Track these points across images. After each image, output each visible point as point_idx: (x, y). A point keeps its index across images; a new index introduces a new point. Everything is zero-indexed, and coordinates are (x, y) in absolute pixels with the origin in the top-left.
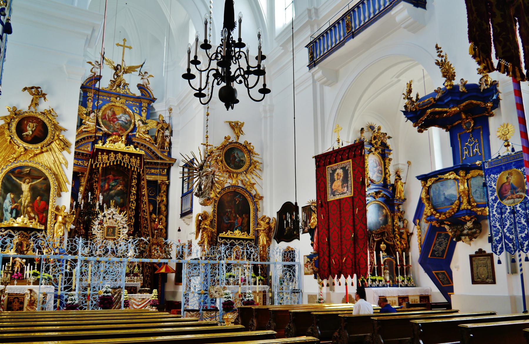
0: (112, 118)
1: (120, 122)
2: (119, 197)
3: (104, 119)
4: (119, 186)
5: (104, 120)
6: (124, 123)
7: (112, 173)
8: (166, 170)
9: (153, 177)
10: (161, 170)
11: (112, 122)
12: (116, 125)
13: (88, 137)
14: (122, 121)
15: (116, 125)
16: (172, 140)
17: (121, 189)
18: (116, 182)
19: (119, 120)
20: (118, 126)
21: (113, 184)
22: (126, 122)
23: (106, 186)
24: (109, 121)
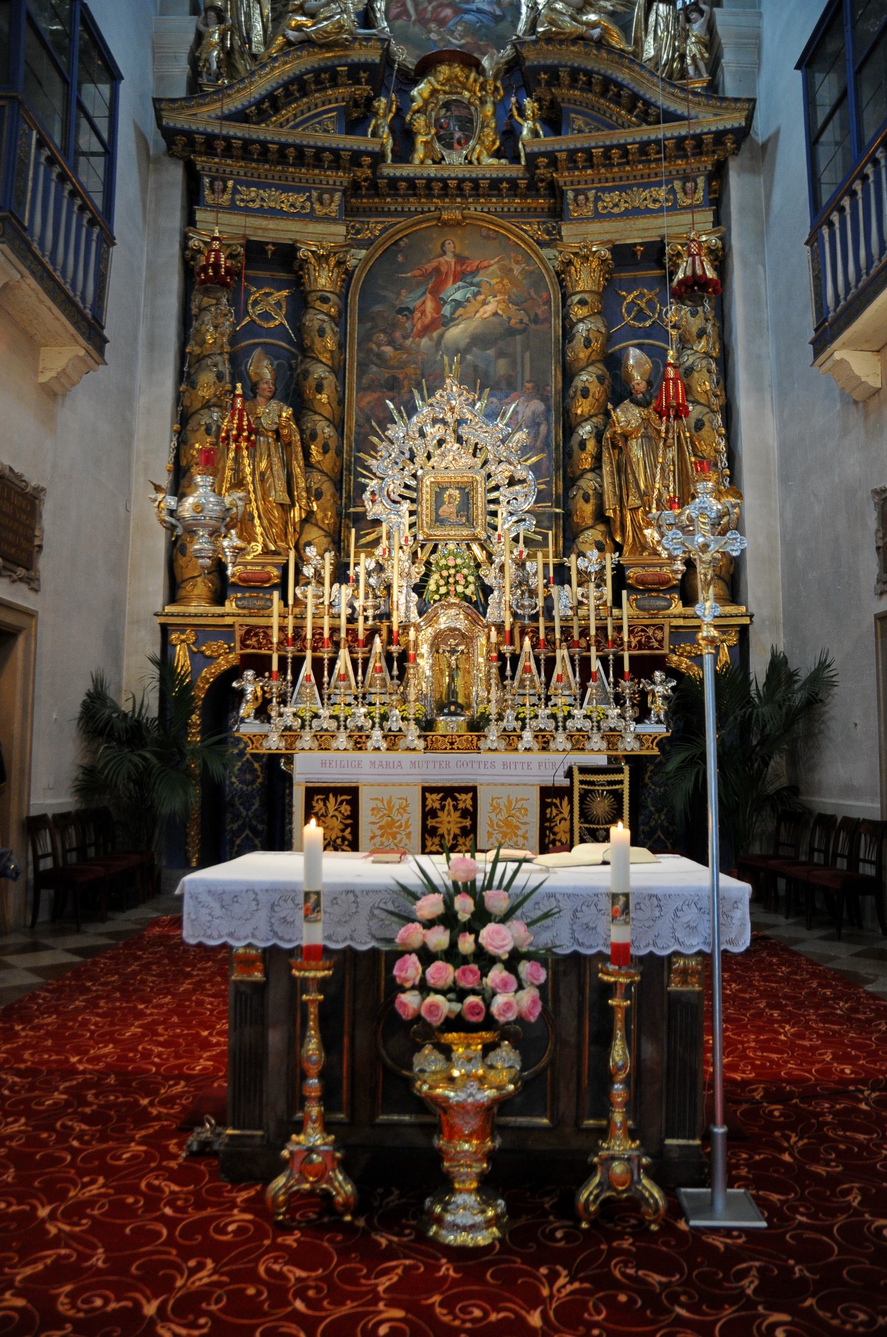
0: (434, 9)
1: (467, 17)
2: (491, 352)
3: (398, 17)
4: (484, 303)
5: (399, 22)
6: (485, 19)
7: (449, 247)
8: (701, 181)
9: (641, 223)
10: (677, 185)
11: (433, 26)
12: (452, 33)
13: (317, 72)
14: (479, 11)
15: (452, 33)
16: (720, 29)
17: (495, 314)
18: (472, 284)
19: (467, 11)
20: (462, 37)
21: (458, 296)
22: (498, 12)
23: (429, 305)
24: (422, 21)
